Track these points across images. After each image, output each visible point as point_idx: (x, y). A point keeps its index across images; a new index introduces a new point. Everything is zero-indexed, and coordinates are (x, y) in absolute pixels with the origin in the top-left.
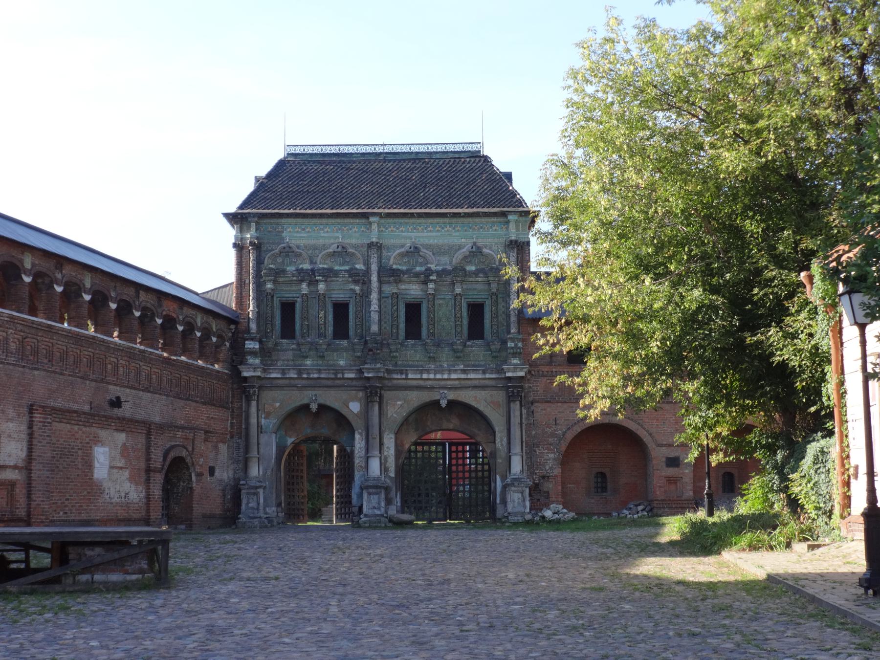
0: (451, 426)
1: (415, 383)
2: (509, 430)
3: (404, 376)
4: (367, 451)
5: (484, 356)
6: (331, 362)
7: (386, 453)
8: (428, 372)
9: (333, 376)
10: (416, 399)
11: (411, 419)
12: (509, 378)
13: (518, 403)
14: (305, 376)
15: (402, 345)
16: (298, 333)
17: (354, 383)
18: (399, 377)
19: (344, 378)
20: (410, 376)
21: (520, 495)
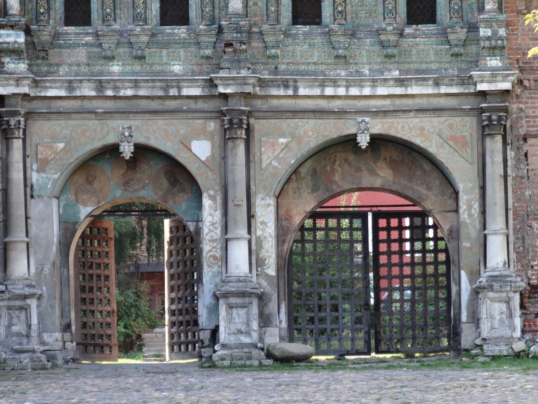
0: (378, 183)
1: (309, 104)
2: (483, 188)
3: (290, 92)
4: (226, 229)
5: (437, 53)
6: (158, 68)
7: (259, 233)
8: (335, 83)
9: (161, 93)
10: (315, 133)
11: (303, 171)
12: (483, 94)
13: (499, 138)
14: (110, 93)
15: (286, 34)
16: (95, 15)
17: (200, 105)
18: (282, 92)
19: (180, 97)
20: (302, 91)
21: (504, 307)
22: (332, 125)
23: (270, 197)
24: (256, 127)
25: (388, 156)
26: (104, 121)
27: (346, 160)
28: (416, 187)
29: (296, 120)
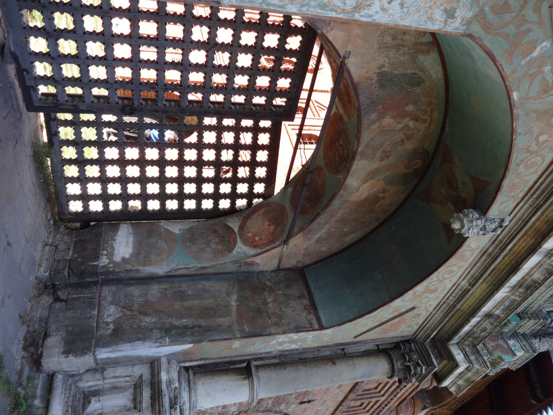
23: (469, 23)
25: (386, 194)
27: (409, 138)
28: (328, 226)
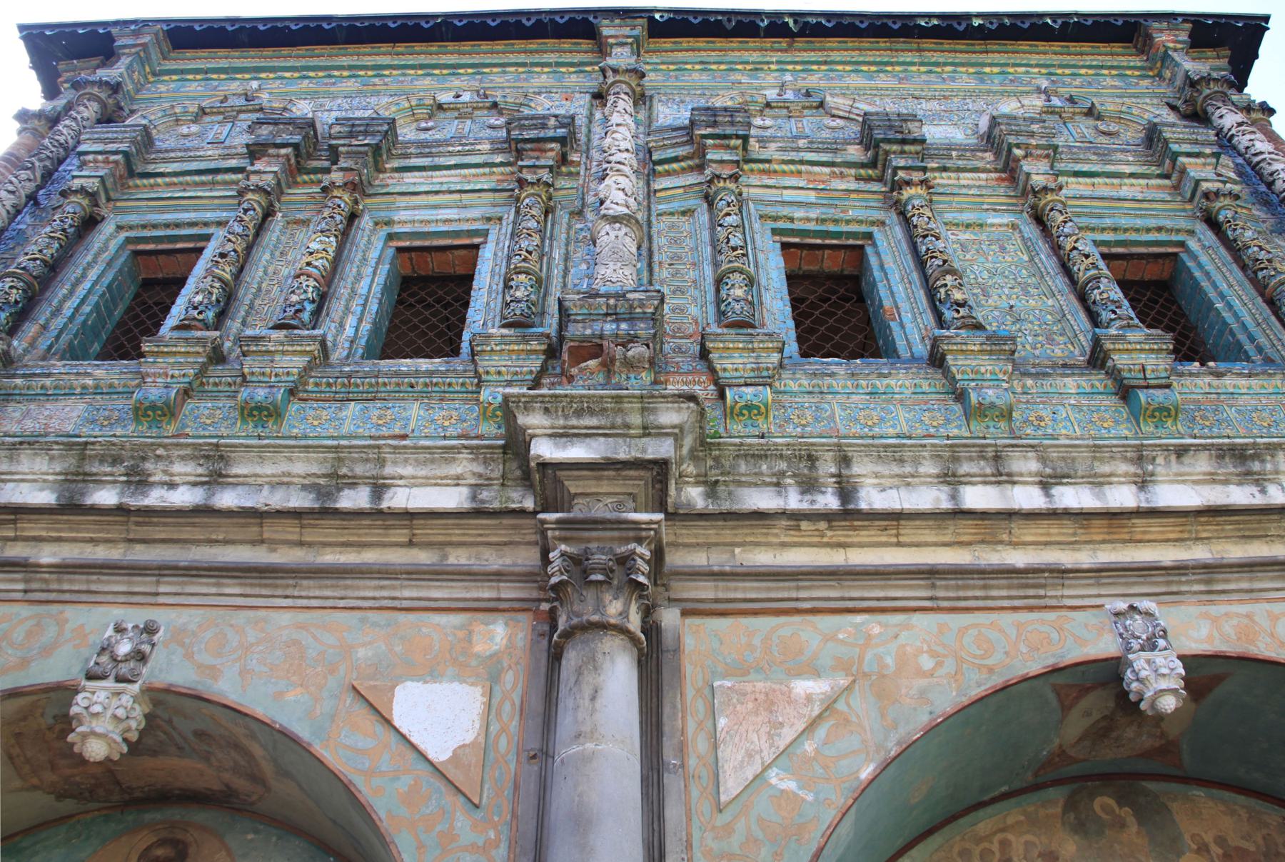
3: (829, 501)
10: (944, 662)
14: (106, 497)
18: (794, 501)
22: (1013, 633)
24: (689, 642)
26: (54, 608)
29: (859, 618)
